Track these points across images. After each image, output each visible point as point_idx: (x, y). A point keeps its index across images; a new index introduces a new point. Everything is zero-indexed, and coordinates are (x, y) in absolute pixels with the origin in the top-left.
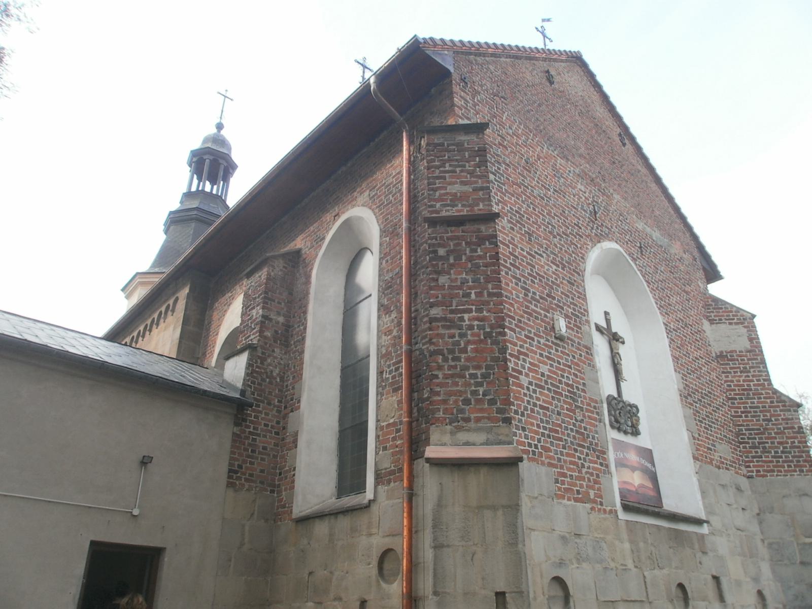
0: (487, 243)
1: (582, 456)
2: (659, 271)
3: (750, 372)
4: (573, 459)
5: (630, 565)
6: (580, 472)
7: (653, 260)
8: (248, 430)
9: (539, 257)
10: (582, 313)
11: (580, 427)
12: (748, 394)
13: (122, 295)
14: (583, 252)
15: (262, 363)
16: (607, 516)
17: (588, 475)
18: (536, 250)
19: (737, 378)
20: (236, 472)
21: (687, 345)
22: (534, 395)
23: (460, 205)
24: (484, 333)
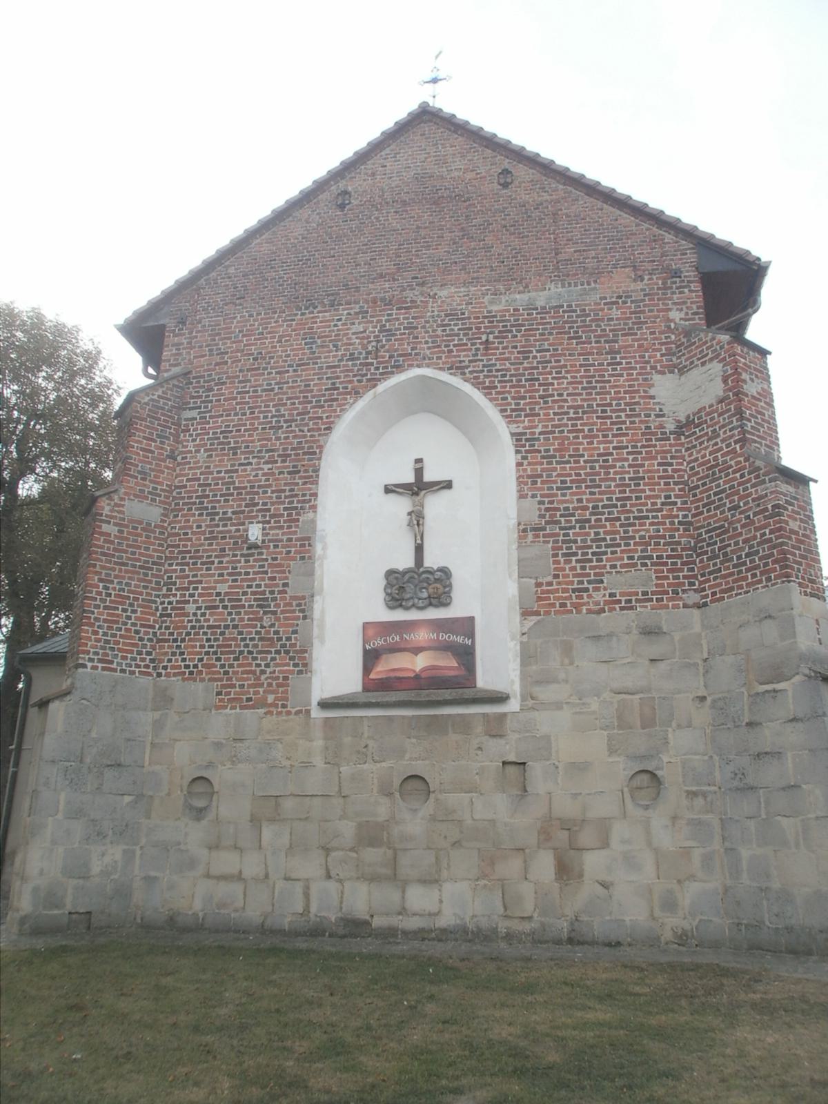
5: (318, 761)
6: (258, 679)
19: (703, 452)
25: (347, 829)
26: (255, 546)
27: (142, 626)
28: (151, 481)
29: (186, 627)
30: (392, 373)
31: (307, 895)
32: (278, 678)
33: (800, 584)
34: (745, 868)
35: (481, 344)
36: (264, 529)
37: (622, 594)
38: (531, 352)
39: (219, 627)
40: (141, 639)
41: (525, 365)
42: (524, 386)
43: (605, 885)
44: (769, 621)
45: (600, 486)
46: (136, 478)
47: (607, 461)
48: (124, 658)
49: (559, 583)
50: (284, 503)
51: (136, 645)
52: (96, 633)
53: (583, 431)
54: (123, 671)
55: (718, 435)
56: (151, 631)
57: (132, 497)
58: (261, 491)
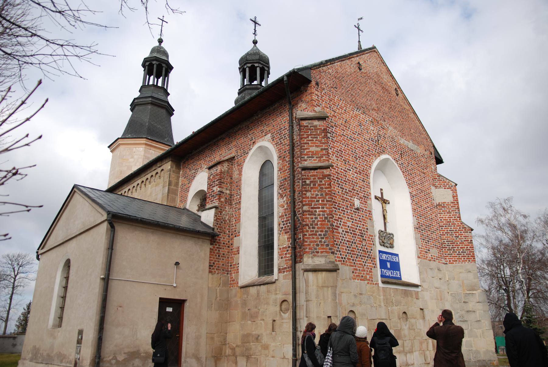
0: (326, 178)
1: (365, 261)
2: (410, 165)
3: (451, 213)
4: (361, 263)
5: (382, 304)
6: (363, 268)
7: (407, 159)
8: (216, 246)
9: (349, 171)
10: (368, 195)
11: (364, 248)
12: (449, 224)
13: (109, 150)
14: (370, 164)
15: (221, 214)
16: (374, 285)
17: (367, 269)
18: (348, 168)
19: (445, 216)
20: (212, 266)
21: (421, 202)
22: (344, 236)
23: (315, 157)
24: (325, 217)
34: (464, 344)
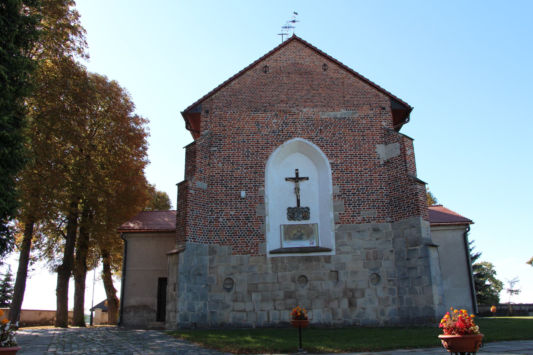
5: (270, 271)
19: (393, 172)
25: (281, 294)
26: (244, 199)
27: (204, 226)
28: (203, 174)
29: (219, 227)
30: (288, 139)
31: (268, 316)
32: (254, 244)
33: (423, 217)
34: (405, 301)
35: (319, 130)
36: (246, 193)
37: (367, 218)
38: (336, 134)
39: (232, 226)
40: (204, 231)
41: (334, 139)
42: (334, 146)
43: (364, 309)
44: (414, 228)
45: (359, 182)
46: (198, 173)
47: (361, 173)
48: (199, 237)
49: (347, 214)
50: (252, 184)
51: (202, 233)
52: (190, 229)
53: (353, 163)
54: (199, 242)
55: (398, 168)
56: (207, 228)
57: (198, 180)
58: (244, 179)
